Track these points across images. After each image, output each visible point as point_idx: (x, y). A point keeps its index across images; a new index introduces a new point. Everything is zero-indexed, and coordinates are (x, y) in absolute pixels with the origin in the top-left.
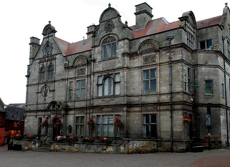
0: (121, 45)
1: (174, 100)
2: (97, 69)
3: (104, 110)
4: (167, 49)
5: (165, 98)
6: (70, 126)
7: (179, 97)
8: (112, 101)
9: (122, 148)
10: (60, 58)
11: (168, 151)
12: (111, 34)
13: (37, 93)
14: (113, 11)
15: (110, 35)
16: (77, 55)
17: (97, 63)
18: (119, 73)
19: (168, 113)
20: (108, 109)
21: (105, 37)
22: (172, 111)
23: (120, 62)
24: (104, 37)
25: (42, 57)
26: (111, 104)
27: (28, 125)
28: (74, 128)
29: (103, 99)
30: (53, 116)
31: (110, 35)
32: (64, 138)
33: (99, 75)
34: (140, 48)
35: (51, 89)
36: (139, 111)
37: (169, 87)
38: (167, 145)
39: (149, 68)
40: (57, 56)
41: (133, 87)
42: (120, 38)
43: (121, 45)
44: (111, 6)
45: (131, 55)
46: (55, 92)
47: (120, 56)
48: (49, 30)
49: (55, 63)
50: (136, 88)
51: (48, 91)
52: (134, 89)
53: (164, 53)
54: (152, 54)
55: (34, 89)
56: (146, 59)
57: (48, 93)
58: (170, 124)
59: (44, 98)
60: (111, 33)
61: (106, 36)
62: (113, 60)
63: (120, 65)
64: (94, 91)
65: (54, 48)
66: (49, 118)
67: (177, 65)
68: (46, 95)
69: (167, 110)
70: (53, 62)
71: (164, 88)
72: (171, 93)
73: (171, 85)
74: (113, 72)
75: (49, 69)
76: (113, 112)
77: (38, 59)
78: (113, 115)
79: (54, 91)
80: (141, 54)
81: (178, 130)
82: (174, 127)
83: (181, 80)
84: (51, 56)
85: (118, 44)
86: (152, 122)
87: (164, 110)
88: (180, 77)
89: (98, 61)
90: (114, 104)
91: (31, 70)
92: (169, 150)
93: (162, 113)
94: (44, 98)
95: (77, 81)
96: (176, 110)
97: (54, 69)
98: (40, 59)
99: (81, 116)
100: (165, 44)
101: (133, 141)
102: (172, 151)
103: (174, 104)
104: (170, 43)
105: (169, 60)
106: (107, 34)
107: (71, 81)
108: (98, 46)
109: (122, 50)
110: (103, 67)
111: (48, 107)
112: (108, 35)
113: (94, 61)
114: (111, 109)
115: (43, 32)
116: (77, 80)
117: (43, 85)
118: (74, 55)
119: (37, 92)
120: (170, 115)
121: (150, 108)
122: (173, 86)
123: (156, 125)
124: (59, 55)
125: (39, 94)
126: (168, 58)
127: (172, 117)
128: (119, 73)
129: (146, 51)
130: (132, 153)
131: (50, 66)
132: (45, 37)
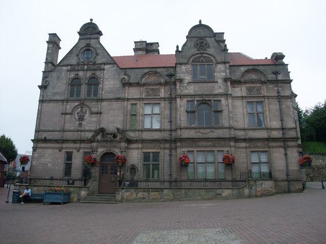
0: (220, 68)
1: (287, 136)
2: (186, 92)
3: (200, 144)
4: (274, 83)
5: (276, 134)
7: (292, 134)
8: (211, 133)
9: (246, 191)
10: (112, 69)
11: (285, 192)
12: (206, 54)
13: (62, 114)
14: (206, 30)
15: (204, 55)
16: (146, 71)
17: (185, 84)
18: (220, 100)
19: (282, 150)
20: (205, 144)
21: (197, 56)
22: (285, 148)
23: (220, 87)
24: (194, 55)
25: (75, 63)
26: (211, 136)
27: (42, 162)
28: (140, 167)
29: (197, 130)
30: (103, 150)
31: (204, 55)
32: (8, 184)
33: (189, 99)
34: (243, 75)
35: (94, 110)
36: (246, 148)
37: (280, 123)
38: (284, 185)
39: (254, 100)
40: (106, 67)
41: (236, 119)
42: (219, 61)
43: (220, 68)
44: (202, 23)
45: (235, 83)
46: (102, 115)
47: (220, 81)
49: (102, 75)
50: (240, 120)
51: (86, 113)
52: (237, 121)
53: (271, 86)
54: (258, 85)
55: (56, 108)
56: (249, 90)
57: (87, 116)
58: (285, 162)
59: (77, 123)
60: (205, 52)
61: (198, 54)
62: (210, 84)
63: (221, 91)
64: (182, 119)
65: (101, 54)
66: (95, 153)
67: (286, 100)
68: (81, 118)
69: (280, 147)
70: (98, 73)
71: (274, 123)
72: (283, 129)
73: (282, 120)
74: (212, 99)
75: (88, 81)
76: (215, 146)
77: (68, 65)
78: (193, 151)
79: (101, 113)
80: (245, 82)
81: (294, 168)
82: (289, 165)
83: (293, 116)
84: (95, 64)
85: (216, 66)
86: (153, 161)
87: (277, 147)
88: (291, 113)
89: (186, 81)
90: (215, 137)
91: (49, 79)
92: (286, 190)
93: (275, 150)
94: (77, 123)
95: (145, 104)
96: (291, 147)
97: (102, 83)
98: (71, 65)
99: (152, 152)
100: (271, 77)
101: (260, 182)
102: (289, 192)
103: (287, 141)
104: (277, 77)
105: (277, 94)
106: (199, 52)
107: (133, 102)
108: (186, 64)
109: (223, 74)
110: (194, 91)
111: (94, 137)
112: (201, 53)
113: (181, 81)
114: (210, 143)
115: (80, 30)
116: (145, 102)
117: (76, 104)
118: (140, 70)
119: (64, 112)
120: (284, 152)
121: (259, 144)
122: (284, 122)
123: (159, 164)
124: (110, 66)
125: (68, 116)
126: (276, 92)
127: (286, 155)
128: (220, 100)
129: (252, 82)
130: (262, 196)
131: (93, 77)
132: (82, 37)
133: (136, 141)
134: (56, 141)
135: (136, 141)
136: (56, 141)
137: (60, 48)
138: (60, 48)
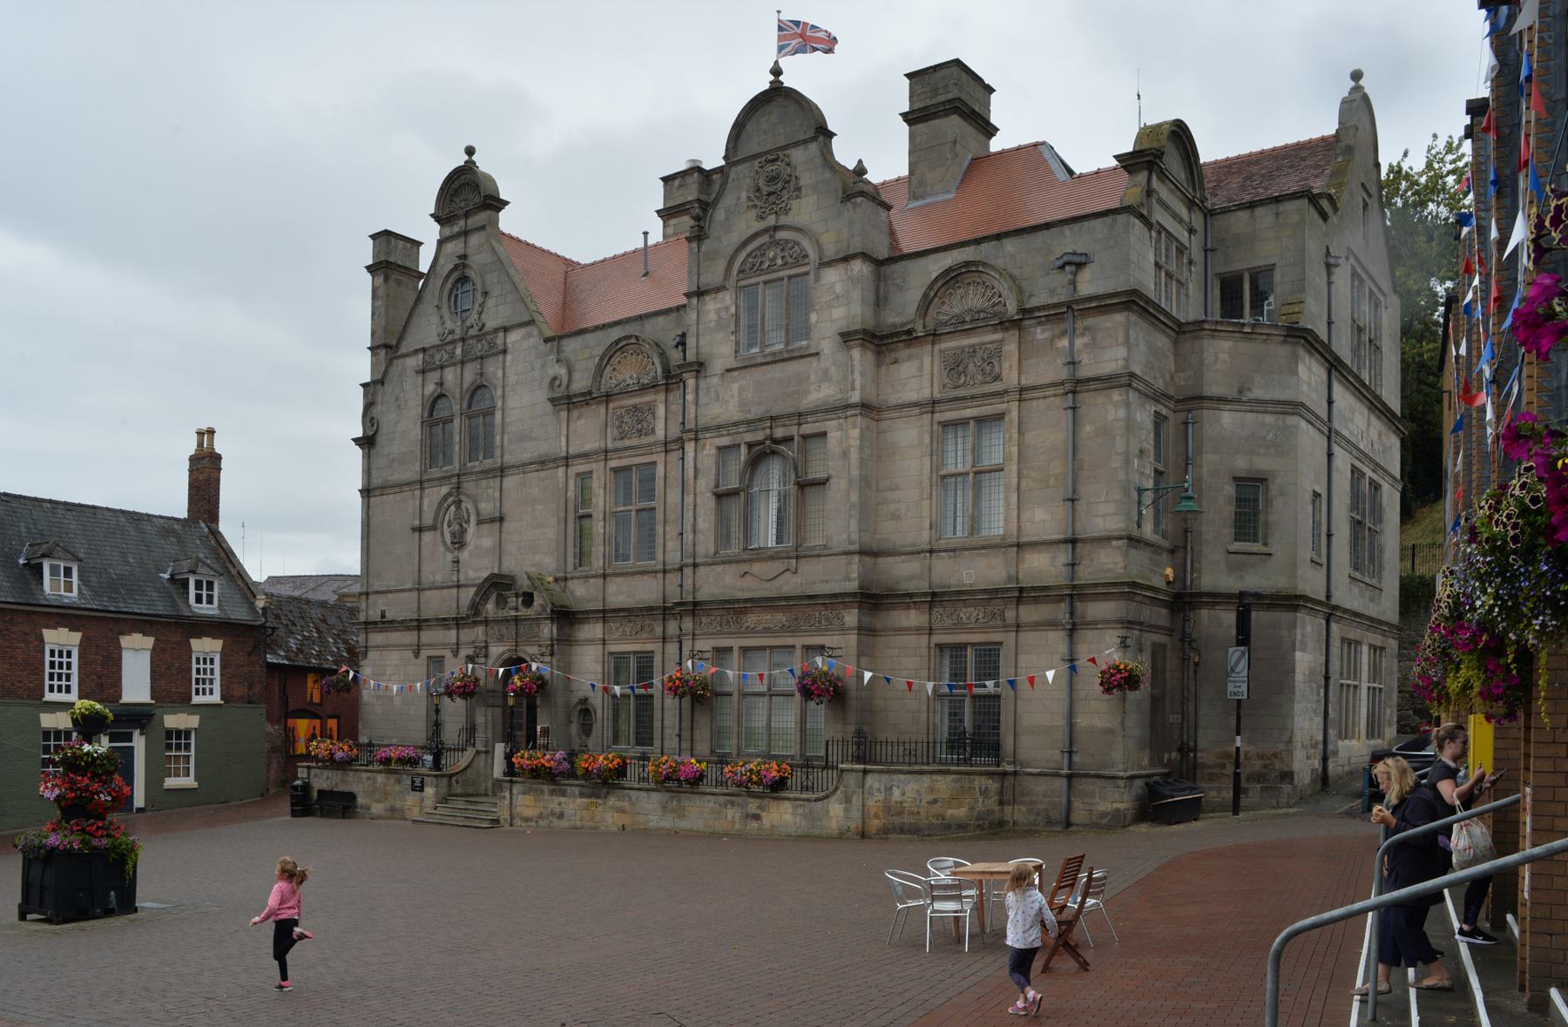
0: (833, 285)
1: (1086, 574)
3: (752, 619)
5: (1044, 567)
6: (585, 701)
7: (1108, 563)
9: (835, 808)
10: (525, 345)
12: (783, 227)
13: (414, 529)
16: (616, 333)
18: (824, 434)
29: (744, 567)
31: (781, 235)
33: (725, 441)
34: (926, 303)
35: (487, 508)
36: (918, 630)
40: (513, 337)
41: (892, 507)
42: (830, 252)
43: (833, 285)
45: (880, 341)
46: (506, 525)
47: (827, 344)
48: (467, 196)
49: (500, 374)
51: (468, 522)
53: (1041, 334)
55: (400, 510)
56: (955, 366)
57: (471, 529)
60: (783, 220)
62: (792, 368)
64: (701, 525)
65: (495, 291)
68: (459, 542)
69: (1052, 624)
70: (493, 368)
74: (793, 431)
76: (791, 630)
77: (416, 352)
79: (501, 519)
80: (934, 336)
85: (818, 279)
87: (1038, 626)
88: (1116, 462)
89: (718, 366)
90: (798, 591)
93: (1028, 637)
94: (450, 557)
96: (1093, 624)
97: (499, 404)
98: (424, 350)
100: (1047, 290)
105: (1064, 374)
106: (762, 225)
107: (582, 468)
108: (717, 290)
109: (838, 313)
111: (476, 607)
112: (766, 230)
113: (699, 367)
114: (781, 618)
116: (613, 464)
117: (445, 490)
118: (599, 334)
119: (417, 523)
121: (967, 614)
122: (1081, 507)
124: (522, 332)
125: (427, 537)
128: (824, 434)
129: (962, 326)
131: (479, 387)
132: (448, 232)
133: (906, 599)
134: (404, 625)
135: (906, 599)
136: (404, 625)
137: (832, 135)
138: (832, 135)
